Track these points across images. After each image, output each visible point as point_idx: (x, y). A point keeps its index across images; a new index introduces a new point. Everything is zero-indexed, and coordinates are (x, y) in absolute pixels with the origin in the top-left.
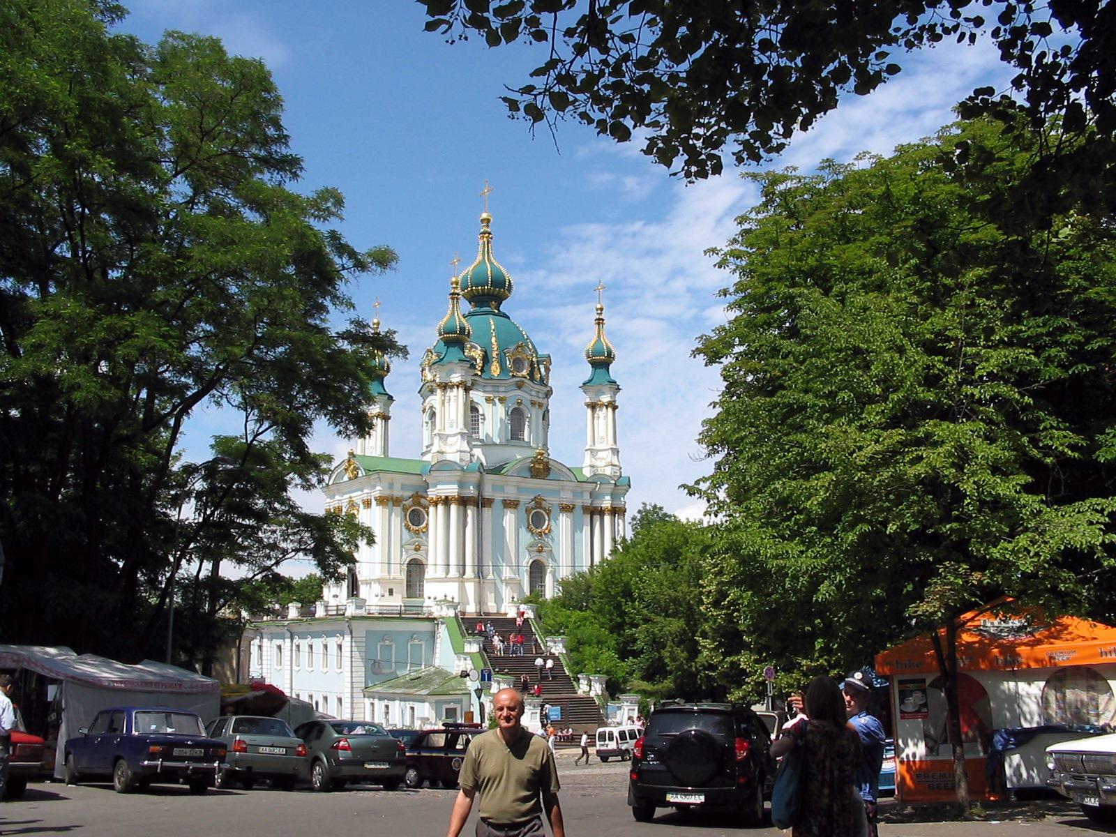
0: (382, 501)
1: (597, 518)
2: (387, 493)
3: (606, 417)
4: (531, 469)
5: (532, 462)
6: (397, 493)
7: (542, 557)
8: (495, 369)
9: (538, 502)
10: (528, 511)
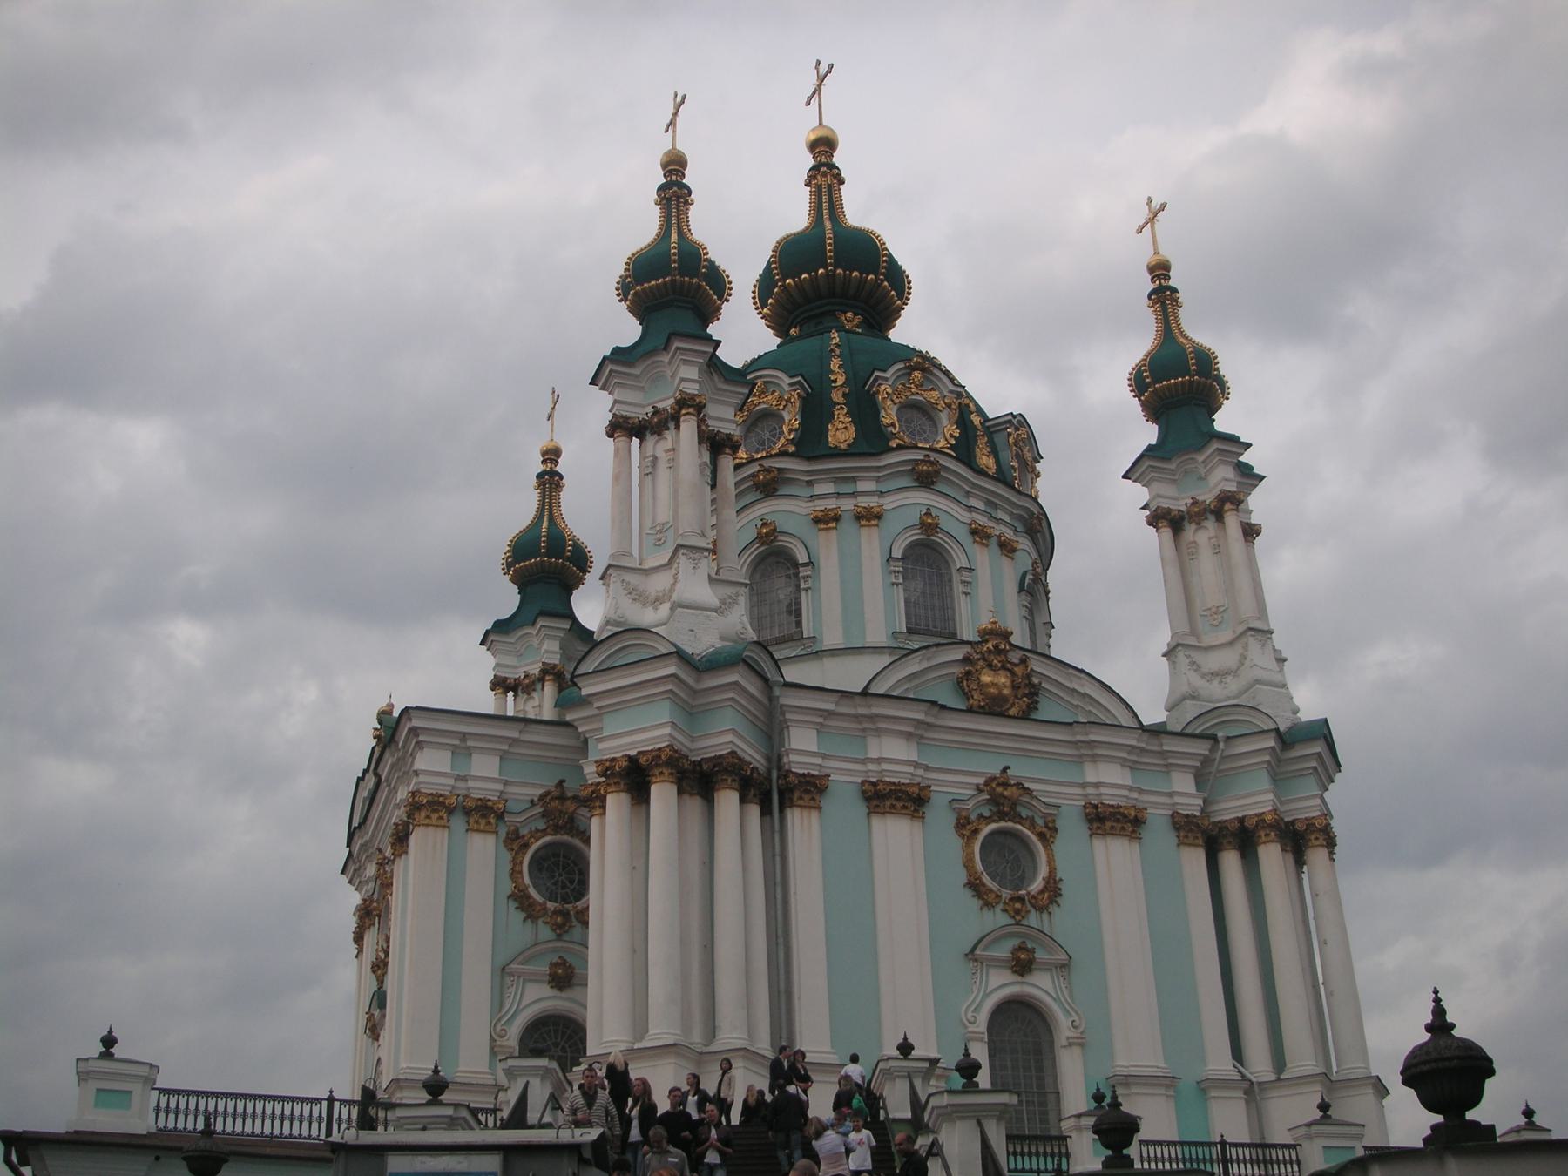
0: (429, 807)
1: (1231, 862)
2: (443, 785)
3: (1218, 549)
4: (964, 683)
5: (967, 660)
6: (485, 773)
7: (1041, 986)
8: (841, 432)
9: (1004, 797)
10: (965, 826)
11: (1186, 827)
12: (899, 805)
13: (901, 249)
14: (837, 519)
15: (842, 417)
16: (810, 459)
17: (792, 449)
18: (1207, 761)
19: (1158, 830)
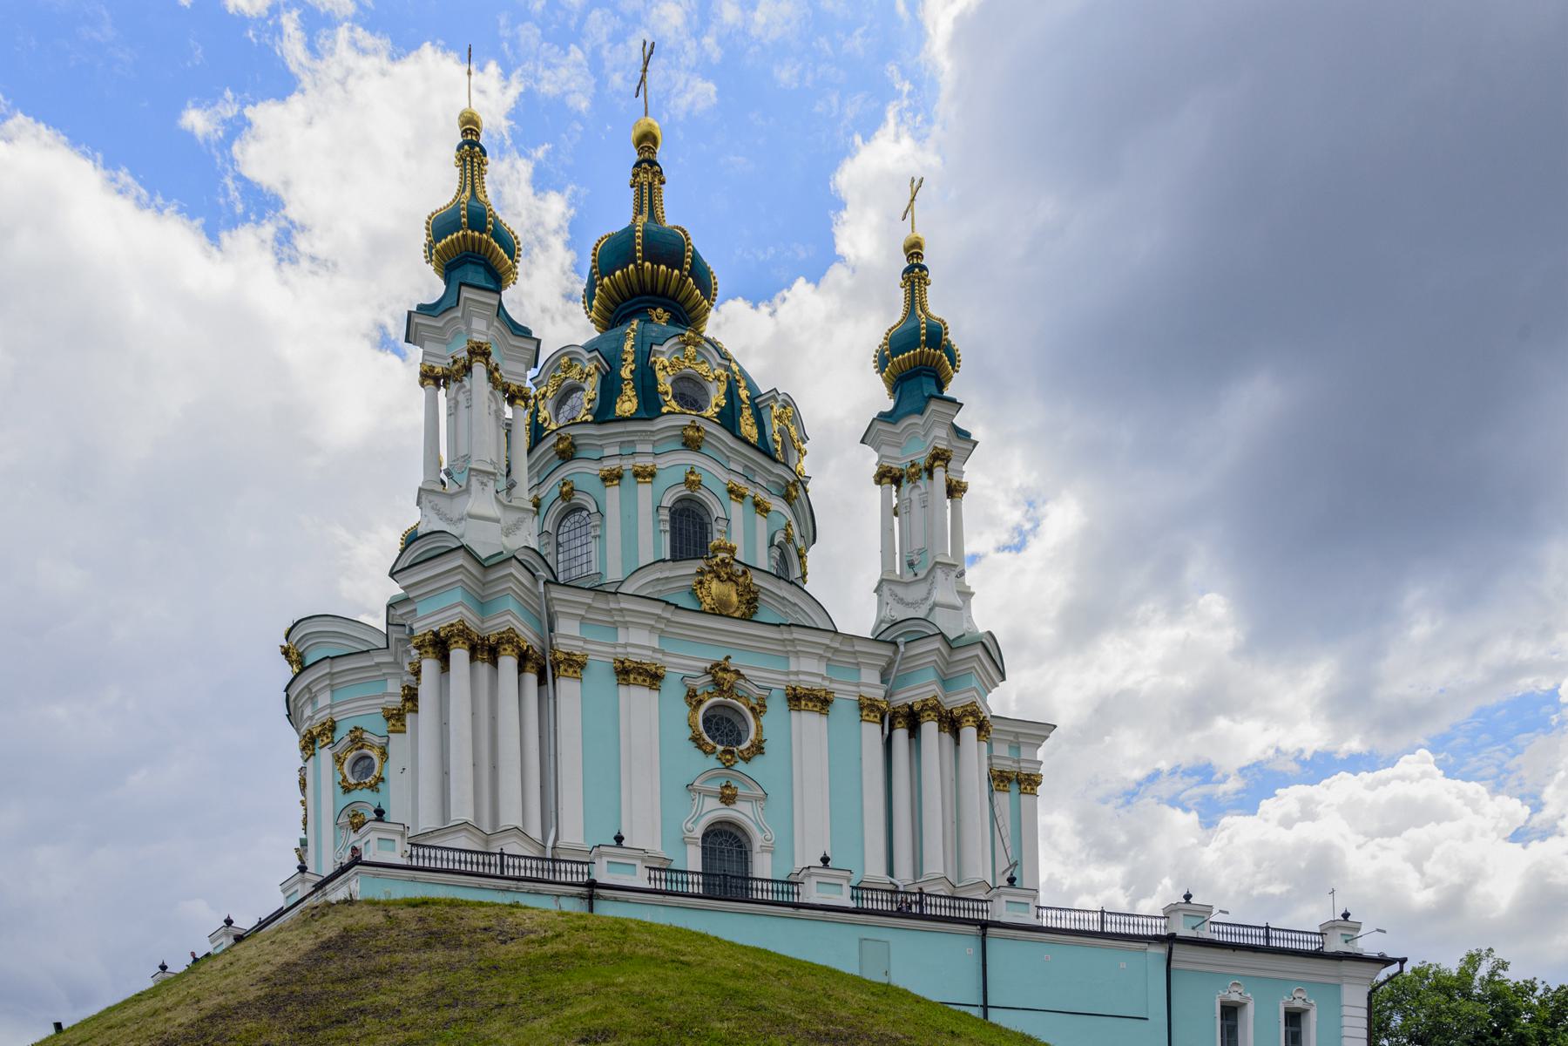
10: (693, 698)
11: (867, 707)
12: (640, 679)
13: (703, 244)
14: (619, 477)
15: (629, 390)
16: (600, 423)
17: (590, 418)
18: (891, 663)
19: (844, 708)
